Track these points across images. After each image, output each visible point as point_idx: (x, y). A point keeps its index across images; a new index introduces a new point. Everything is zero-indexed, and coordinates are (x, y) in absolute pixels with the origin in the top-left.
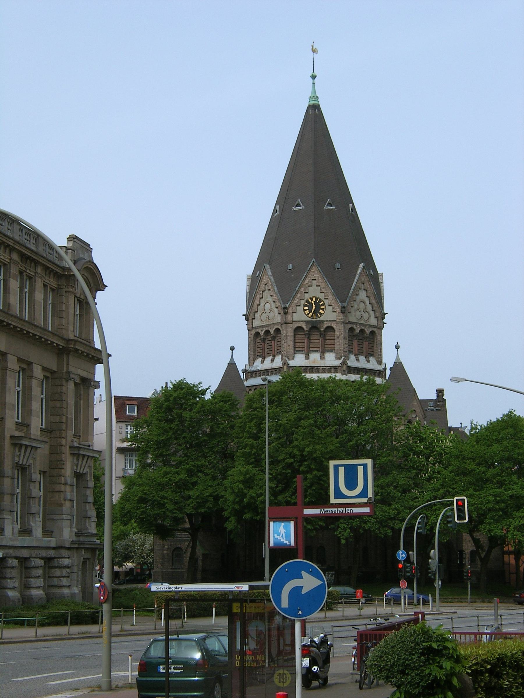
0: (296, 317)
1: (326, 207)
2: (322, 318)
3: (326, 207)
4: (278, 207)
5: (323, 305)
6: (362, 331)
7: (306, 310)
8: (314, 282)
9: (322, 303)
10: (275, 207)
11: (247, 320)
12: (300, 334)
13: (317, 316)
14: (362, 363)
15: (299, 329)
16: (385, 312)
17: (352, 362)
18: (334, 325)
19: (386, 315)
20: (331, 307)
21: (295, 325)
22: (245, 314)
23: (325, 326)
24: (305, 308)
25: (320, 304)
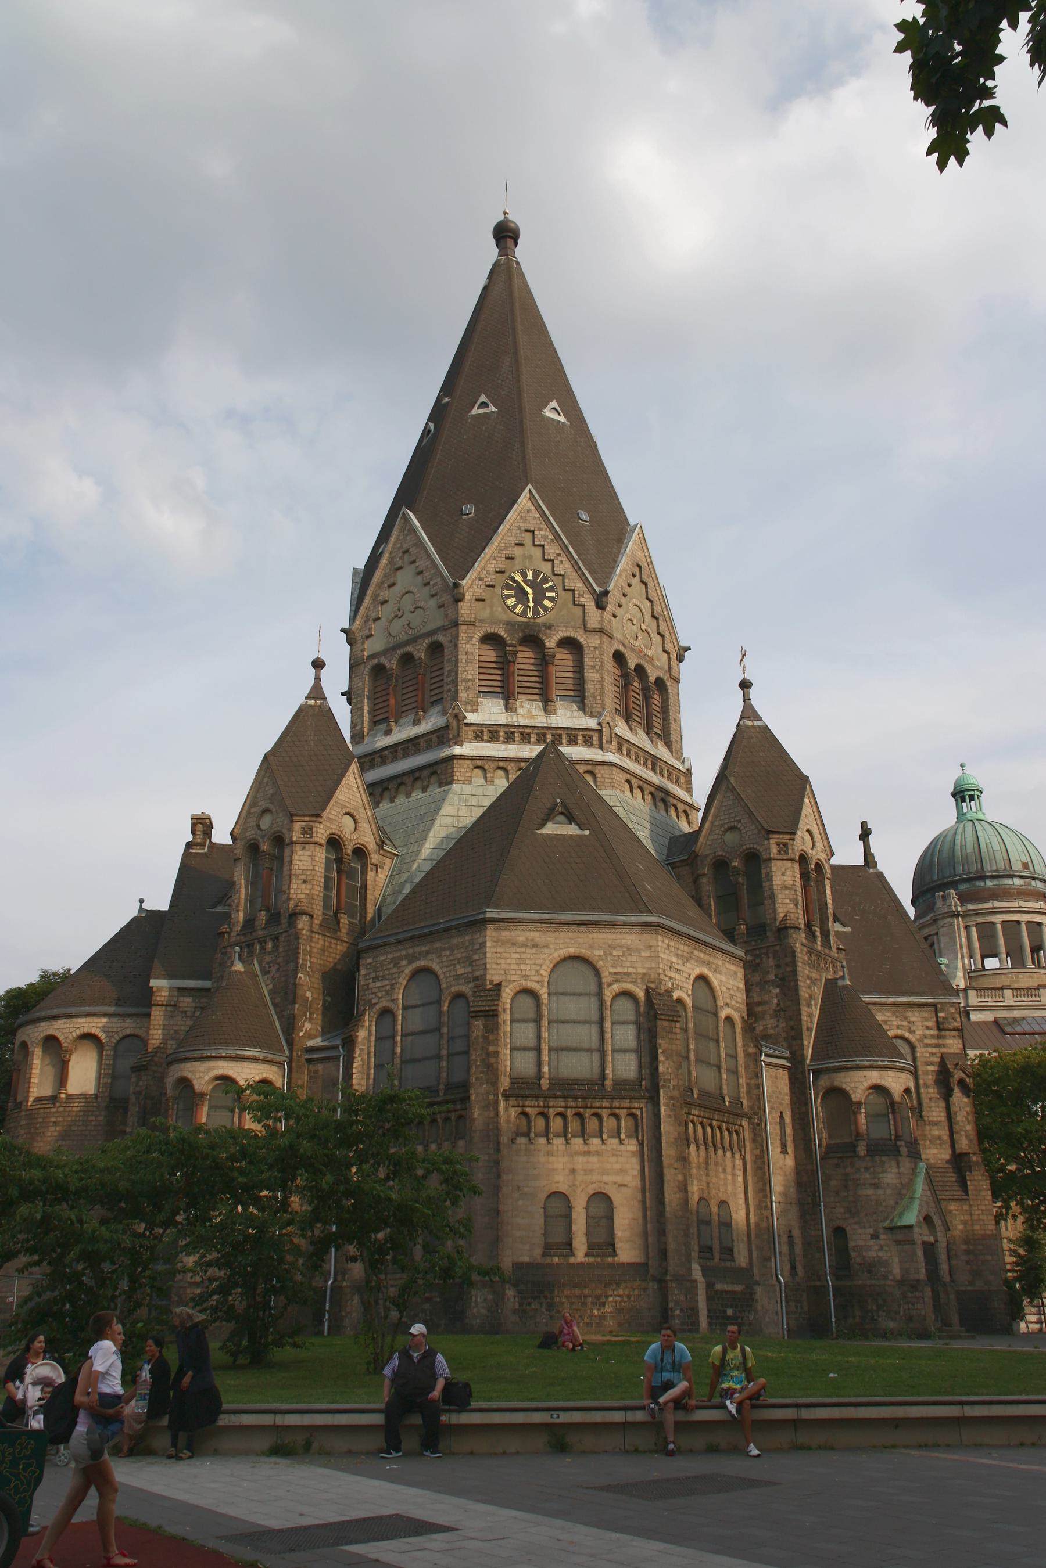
4: (432, 425)
5: (551, 589)
7: (509, 597)
9: (550, 584)
10: (427, 424)
11: (350, 642)
14: (640, 738)
18: (582, 638)
19: (687, 654)
22: (346, 626)
25: (545, 586)
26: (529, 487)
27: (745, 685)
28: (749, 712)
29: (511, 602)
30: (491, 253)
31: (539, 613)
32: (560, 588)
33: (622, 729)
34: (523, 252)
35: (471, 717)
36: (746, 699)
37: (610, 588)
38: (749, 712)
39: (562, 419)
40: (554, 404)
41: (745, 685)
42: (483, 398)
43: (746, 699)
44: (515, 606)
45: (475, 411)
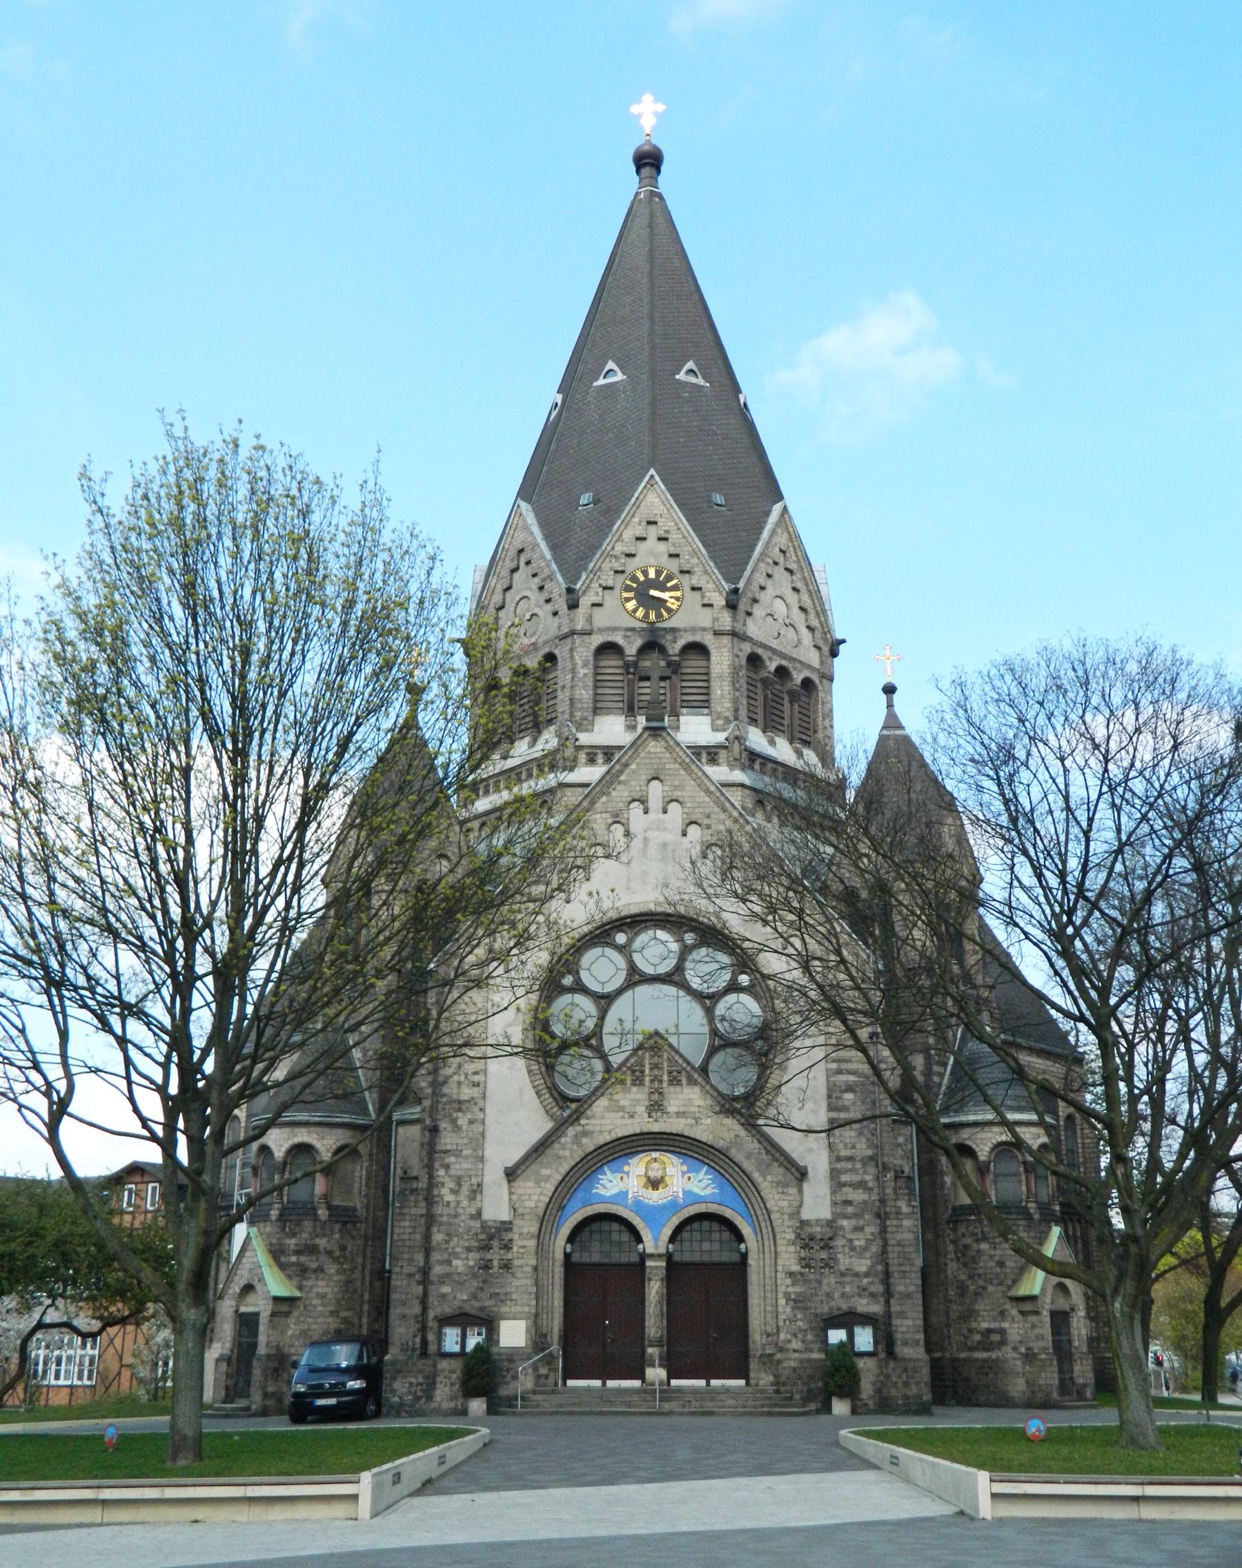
0: (601, 618)
1: (681, 376)
2: (673, 623)
3: (681, 376)
6: (782, 672)
7: (628, 600)
8: (652, 528)
9: (674, 582)
12: (611, 664)
13: (659, 616)
14: (783, 751)
15: (608, 649)
16: (839, 636)
17: (756, 739)
18: (708, 640)
19: (842, 647)
20: (697, 594)
21: (597, 640)
23: (681, 643)
24: (626, 595)
26: (652, 471)
27: (889, 690)
28: (892, 722)
29: (631, 605)
30: (629, 182)
31: (662, 616)
32: (687, 589)
33: (756, 739)
34: (666, 182)
35: (584, 738)
36: (890, 705)
37: (741, 585)
38: (892, 722)
39: (700, 381)
40: (690, 365)
41: (889, 690)
42: (611, 365)
43: (890, 705)
44: (635, 611)
45: (601, 382)
